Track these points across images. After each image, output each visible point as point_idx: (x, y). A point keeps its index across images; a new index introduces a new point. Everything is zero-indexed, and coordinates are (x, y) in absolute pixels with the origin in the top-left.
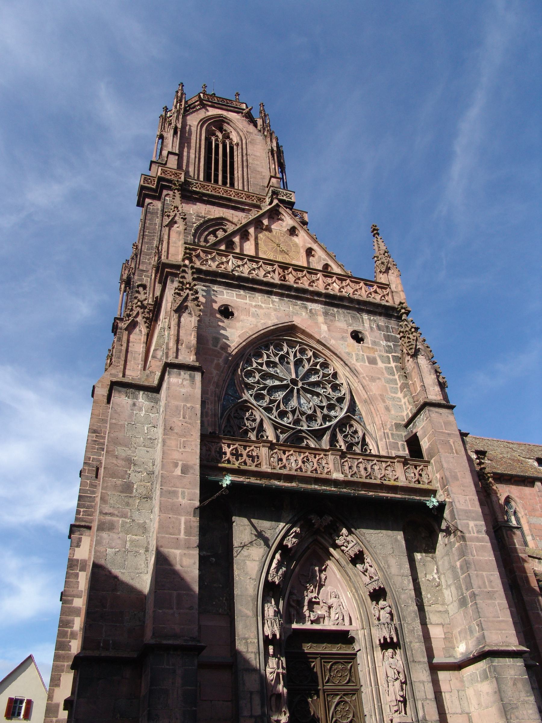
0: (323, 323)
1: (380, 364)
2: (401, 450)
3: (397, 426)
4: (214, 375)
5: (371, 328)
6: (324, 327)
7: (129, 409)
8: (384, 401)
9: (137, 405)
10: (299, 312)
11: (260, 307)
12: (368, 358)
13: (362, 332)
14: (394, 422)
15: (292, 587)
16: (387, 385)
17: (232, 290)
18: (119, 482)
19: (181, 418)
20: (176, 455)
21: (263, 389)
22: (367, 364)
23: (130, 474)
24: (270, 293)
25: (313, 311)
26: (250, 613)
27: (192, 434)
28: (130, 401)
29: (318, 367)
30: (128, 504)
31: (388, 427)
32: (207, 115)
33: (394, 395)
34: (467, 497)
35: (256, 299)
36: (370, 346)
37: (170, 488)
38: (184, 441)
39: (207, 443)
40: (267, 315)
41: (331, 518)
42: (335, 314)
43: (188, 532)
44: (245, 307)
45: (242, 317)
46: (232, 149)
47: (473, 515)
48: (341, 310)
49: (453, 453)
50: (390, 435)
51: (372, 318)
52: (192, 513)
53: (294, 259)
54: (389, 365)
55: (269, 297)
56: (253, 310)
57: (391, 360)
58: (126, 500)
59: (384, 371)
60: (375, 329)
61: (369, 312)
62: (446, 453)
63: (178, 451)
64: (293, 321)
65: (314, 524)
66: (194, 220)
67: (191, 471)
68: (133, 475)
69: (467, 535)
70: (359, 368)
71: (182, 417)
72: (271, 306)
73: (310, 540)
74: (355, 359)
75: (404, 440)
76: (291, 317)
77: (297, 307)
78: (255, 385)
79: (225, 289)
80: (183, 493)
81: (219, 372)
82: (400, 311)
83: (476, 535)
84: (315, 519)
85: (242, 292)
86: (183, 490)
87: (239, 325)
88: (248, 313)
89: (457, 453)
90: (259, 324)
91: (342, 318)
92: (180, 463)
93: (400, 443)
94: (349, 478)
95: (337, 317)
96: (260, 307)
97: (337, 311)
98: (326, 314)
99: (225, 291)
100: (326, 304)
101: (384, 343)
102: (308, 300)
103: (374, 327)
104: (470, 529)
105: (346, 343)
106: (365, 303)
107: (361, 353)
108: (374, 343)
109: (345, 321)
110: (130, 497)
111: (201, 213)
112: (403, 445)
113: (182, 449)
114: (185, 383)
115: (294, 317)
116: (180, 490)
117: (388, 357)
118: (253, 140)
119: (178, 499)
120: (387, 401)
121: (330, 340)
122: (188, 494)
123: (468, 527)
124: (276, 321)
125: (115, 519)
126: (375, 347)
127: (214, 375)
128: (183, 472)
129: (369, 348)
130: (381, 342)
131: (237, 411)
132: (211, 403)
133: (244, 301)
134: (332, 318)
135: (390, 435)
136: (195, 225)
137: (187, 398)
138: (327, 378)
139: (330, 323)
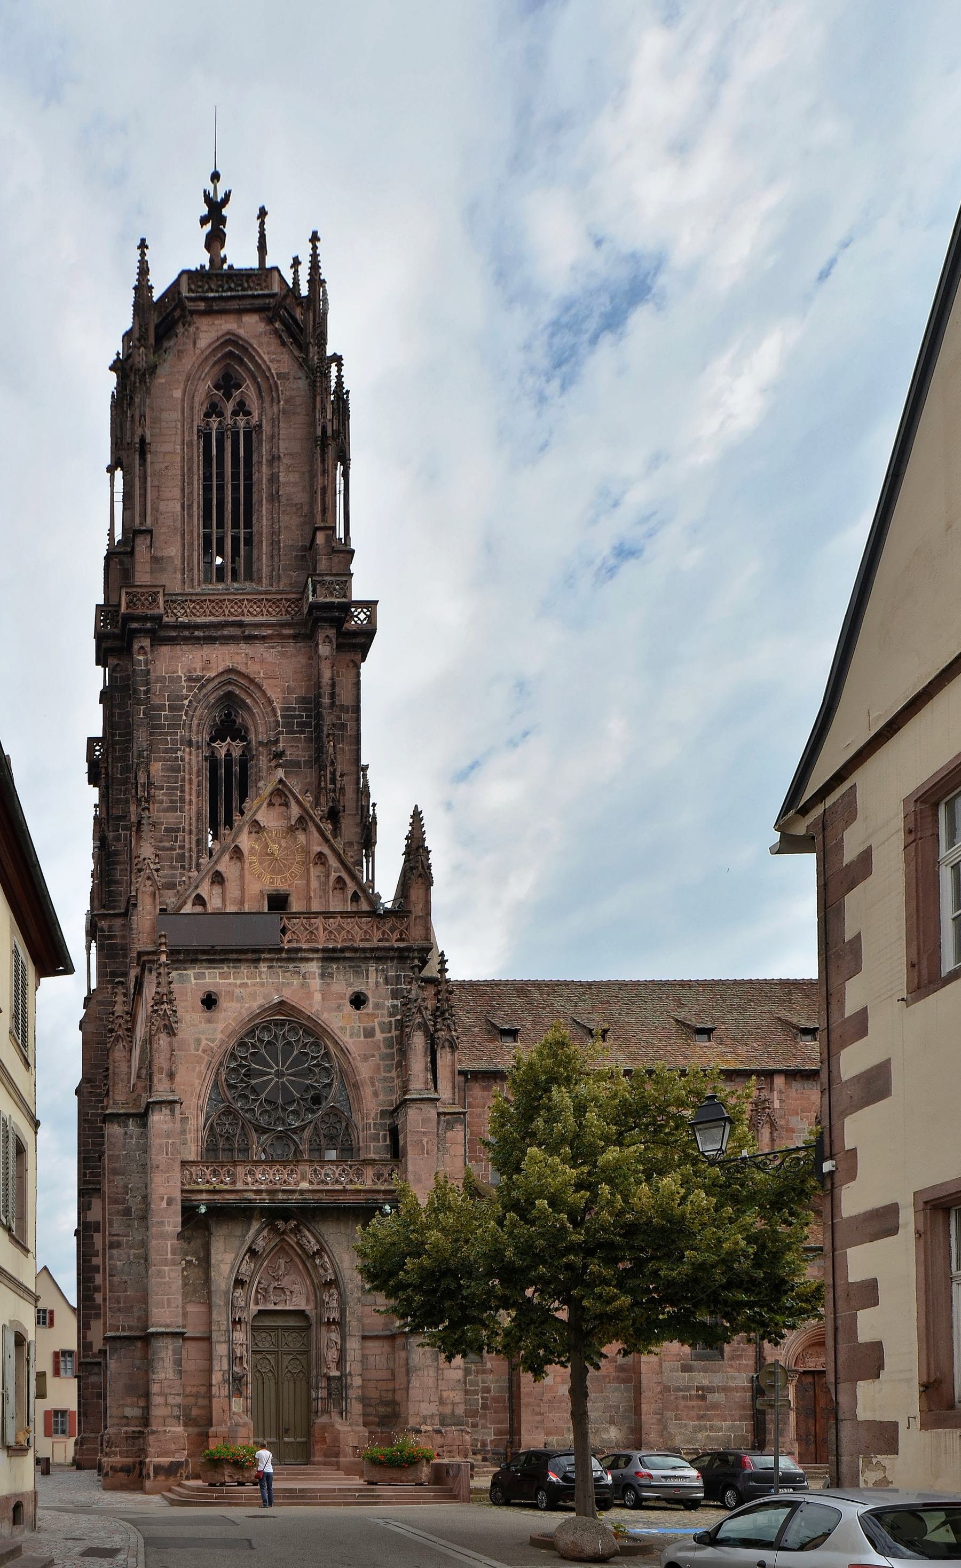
3: (383, 1113)
14: (380, 1109)
17: (214, 968)
26: (222, 1303)
31: (373, 1115)
50: (372, 1125)
61: (378, 959)
73: (278, 1240)
93: (381, 1133)
131: (219, 1116)
133: (228, 981)
135: (372, 1125)
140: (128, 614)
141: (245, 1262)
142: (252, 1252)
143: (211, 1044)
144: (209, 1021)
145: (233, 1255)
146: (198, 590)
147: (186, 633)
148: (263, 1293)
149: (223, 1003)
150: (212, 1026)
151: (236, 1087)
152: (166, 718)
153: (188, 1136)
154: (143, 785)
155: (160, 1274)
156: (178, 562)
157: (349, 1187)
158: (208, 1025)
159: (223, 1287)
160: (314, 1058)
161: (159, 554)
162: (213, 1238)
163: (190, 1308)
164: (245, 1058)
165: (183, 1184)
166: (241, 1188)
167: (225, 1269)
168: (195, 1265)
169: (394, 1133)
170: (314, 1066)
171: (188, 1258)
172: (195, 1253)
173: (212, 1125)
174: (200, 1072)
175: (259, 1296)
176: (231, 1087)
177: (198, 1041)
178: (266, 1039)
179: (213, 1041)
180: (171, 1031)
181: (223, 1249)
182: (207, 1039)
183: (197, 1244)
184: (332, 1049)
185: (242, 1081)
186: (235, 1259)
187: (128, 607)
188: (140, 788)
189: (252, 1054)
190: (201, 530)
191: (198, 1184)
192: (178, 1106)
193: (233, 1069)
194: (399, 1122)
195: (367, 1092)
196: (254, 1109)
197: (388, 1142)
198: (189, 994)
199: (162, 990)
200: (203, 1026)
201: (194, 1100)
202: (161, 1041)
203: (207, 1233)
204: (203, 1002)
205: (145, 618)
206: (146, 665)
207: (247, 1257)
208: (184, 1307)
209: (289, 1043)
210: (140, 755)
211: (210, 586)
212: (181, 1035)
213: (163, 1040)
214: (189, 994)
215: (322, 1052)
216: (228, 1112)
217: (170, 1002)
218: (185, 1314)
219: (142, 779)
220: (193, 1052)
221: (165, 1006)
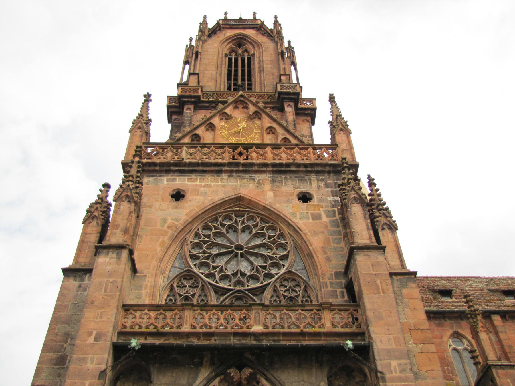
0: (269, 190)
1: (325, 219)
2: (339, 297)
3: (337, 274)
4: (158, 251)
5: (319, 187)
6: (270, 194)
7: (74, 291)
9: (83, 286)
10: (246, 185)
11: (209, 186)
12: (312, 215)
13: (309, 192)
14: (334, 271)
16: (330, 237)
19: (103, 292)
20: (92, 325)
21: (208, 258)
22: (311, 220)
23: (66, 348)
24: (220, 172)
25: (261, 181)
27: (110, 304)
28: (77, 284)
29: (265, 231)
31: (328, 276)
32: (226, 37)
33: (336, 246)
34: (391, 336)
35: (205, 180)
36: (316, 203)
37: (81, 356)
38: (101, 312)
39: (133, 312)
41: (251, 370)
42: (282, 181)
44: (194, 188)
45: (190, 198)
46: (249, 59)
47: (397, 353)
48: (288, 176)
49: (379, 293)
50: (328, 284)
51: (321, 178)
52: (97, 377)
53: (255, 139)
54: (334, 218)
55: (219, 176)
56: (202, 189)
57: (337, 213)
58: (58, 371)
59: (329, 225)
60: (323, 187)
62: (371, 293)
63: (95, 321)
64: (241, 193)
65: (232, 378)
67: (103, 338)
69: (388, 376)
70: (302, 225)
71: (103, 291)
72: (220, 183)
74: (298, 218)
75: (344, 286)
76: (238, 190)
77: (245, 180)
78: (200, 255)
80: (92, 359)
81: (162, 248)
82: (343, 165)
83: (398, 374)
84: (233, 372)
85: (193, 176)
86: (92, 356)
88: (196, 192)
89: (383, 292)
90: (206, 201)
91: (289, 183)
92: (95, 332)
93: (339, 291)
94: (270, 330)
95: (284, 183)
96: (209, 186)
97: (285, 178)
98: (273, 181)
99: (177, 178)
101: (331, 199)
102: (256, 172)
103: (322, 185)
104: (392, 368)
105: (291, 205)
106: (312, 165)
107: (306, 211)
108: (321, 200)
109: (292, 184)
110: (63, 368)
112: (342, 292)
113: (99, 320)
114: (113, 261)
115: (241, 189)
116: (90, 356)
117: (334, 211)
118: (267, 48)
119: (86, 364)
120: (328, 252)
121: (275, 205)
122: (97, 359)
123: (390, 367)
124: (224, 195)
126: (321, 204)
127: (158, 251)
128: (96, 339)
129: (314, 205)
130: (328, 198)
132: (152, 276)
134: (279, 184)
135: (328, 284)
137: (110, 274)
138: (272, 240)
139: (277, 189)
140: (182, 95)
143: (176, 223)
149: (189, 196)
150: (177, 210)
153: (144, 291)
158: (174, 210)
164: (208, 237)
174: (163, 242)
176: (193, 257)
177: (165, 221)
179: (177, 220)
182: (172, 219)
184: (286, 230)
185: (204, 253)
195: (320, 258)
197: (346, 298)
205: (191, 97)
220: (159, 227)
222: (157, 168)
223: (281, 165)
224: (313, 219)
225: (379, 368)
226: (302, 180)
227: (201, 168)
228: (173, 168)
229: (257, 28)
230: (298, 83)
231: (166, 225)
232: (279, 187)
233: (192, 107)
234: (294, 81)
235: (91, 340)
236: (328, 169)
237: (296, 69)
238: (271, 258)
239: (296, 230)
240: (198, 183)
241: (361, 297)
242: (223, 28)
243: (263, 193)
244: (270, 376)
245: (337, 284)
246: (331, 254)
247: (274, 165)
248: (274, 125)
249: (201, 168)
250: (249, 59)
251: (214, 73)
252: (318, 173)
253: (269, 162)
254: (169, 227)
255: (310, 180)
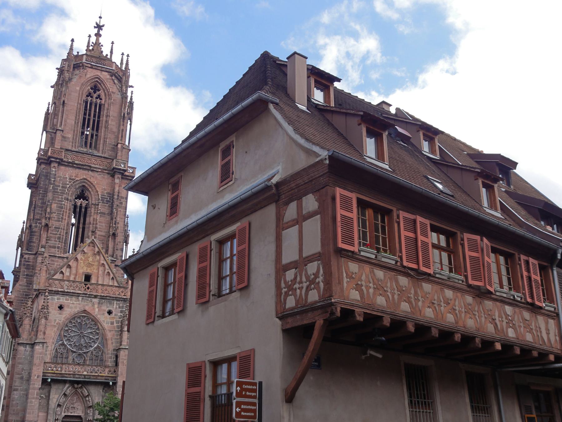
1: (115, 324)
3: (114, 350)
5: (116, 307)
6: (97, 310)
8: (112, 340)
12: (111, 322)
15: (67, 403)
18: (20, 376)
20: (36, 373)
22: (110, 325)
26: (52, 413)
28: (24, 349)
30: (22, 383)
31: (111, 350)
32: (87, 78)
40: (76, 307)
43: (37, 395)
46: (100, 106)
55: (78, 298)
56: (71, 305)
59: (116, 327)
66: (68, 182)
68: (24, 374)
73: (74, 390)
77: (88, 302)
79: (61, 297)
80: (37, 384)
87: (64, 313)
88: (68, 306)
90: (72, 312)
93: (113, 356)
98: (99, 303)
99: (61, 298)
100: (100, 298)
101: (119, 314)
108: (116, 315)
111: (73, 176)
112: (114, 357)
117: (119, 320)
125: (18, 387)
128: (37, 377)
136: (68, 186)
137: (41, 353)
141: (62, 398)
142: (65, 395)
144: (60, 314)
145: (58, 396)
146: (77, 150)
147: (71, 165)
148: (68, 409)
151: (67, 336)
152: (60, 190)
153: (48, 352)
154: (48, 213)
155: (31, 402)
156: (71, 140)
157: (100, 374)
159: (53, 407)
160: (94, 329)
161: (65, 136)
162: (52, 389)
163: (40, 414)
165: (44, 370)
166: (63, 373)
167: (55, 400)
168: (44, 398)
169: (117, 357)
170: (93, 331)
171: (42, 396)
172: (45, 394)
173: (56, 349)
174: (55, 331)
175: (66, 410)
176: (65, 336)
177: (55, 320)
178: (79, 321)
179: (60, 321)
180: (46, 319)
181: (55, 393)
183: (46, 390)
184: (100, 327)
185: (69, 334)
186: (59, 397)
187: (51, 153)
188: (47, 213)
189: (73, 325)
190: (81, 130)
191: (48, 370)
192: (45, 344)
193: (66, 330)
194: (118, 354)
195: (109, 342)
196: (71, 344)
197: (115, 359)
198: (54, 304)
199: (45, 304)
200: (58, 315)
201: (51, 340)
202: (42, 321)
203: (50, 387)
204: (59, 307)
205: (57, 158)
206: (55, 172)
207: (63, 396)
208: (38, 413)
209: (86, 323)
210: (49, 201)
211: (82, 149)
212: (50, 318)
213: (43, 321)
214: (54, 304)
215: (97, 327)
216: (63, 344)
217: (47, 309)
218: (38, 416)
219: (48, 210)
221: (45, 310)
222: (53, 292)
223: (103, 296)
224: (111, 324)
225: (117, 391)
226: (110, 303)
227: (71, 294)
228: (60, 293)
229: (111, 73)
230: (128, 146)
231: (56, 323)
232: (101, 306)
233: (56, 165)
234: (127, 143)
235: (36, 377)
236: (122, 299)
237: (131, 125)
238: (93, 339)
239: (104, 329)
240: (69, 302)
241: (119, 365)
242: (86, 66)
243: (94, 309)
244: (86, 387)
245: (113, 353)
246: (114, 341)
247: (101, 296)
248: (105, 263)
249: (71, 294)
250: (100, 106)
251: (74, 123)
252: (117, 300)
253: (99, 295)
254: (57, 324)
255: (114, 303)
